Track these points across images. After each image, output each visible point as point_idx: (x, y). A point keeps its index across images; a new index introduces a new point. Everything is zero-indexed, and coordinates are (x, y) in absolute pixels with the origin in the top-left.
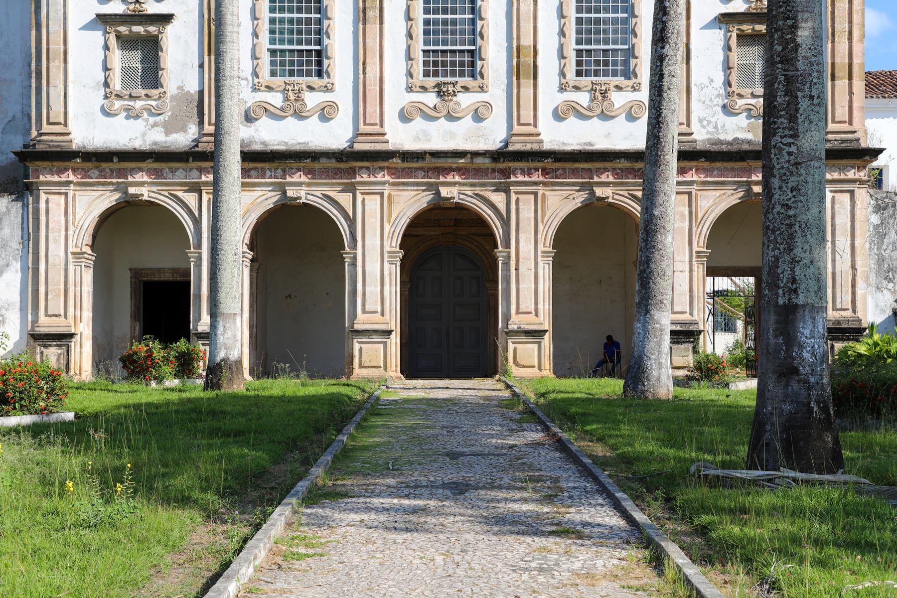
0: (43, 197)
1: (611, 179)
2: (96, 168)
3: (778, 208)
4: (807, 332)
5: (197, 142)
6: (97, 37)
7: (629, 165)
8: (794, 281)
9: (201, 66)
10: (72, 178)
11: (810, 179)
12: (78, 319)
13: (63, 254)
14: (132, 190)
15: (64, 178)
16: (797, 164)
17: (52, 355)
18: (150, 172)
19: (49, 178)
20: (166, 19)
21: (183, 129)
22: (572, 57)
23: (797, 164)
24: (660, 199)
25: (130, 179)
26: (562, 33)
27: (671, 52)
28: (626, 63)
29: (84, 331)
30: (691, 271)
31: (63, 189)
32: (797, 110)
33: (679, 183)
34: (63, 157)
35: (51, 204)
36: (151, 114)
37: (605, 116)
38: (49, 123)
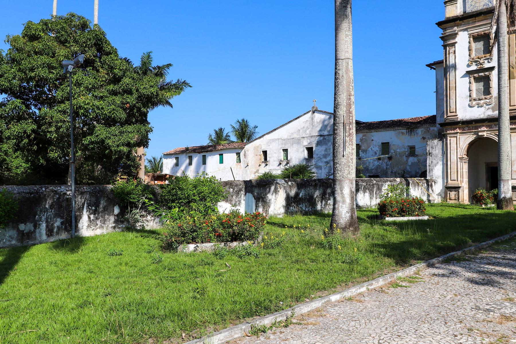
2: (467, 127)
6: (467, 79)
10: (458, 131)
12: (462, 182)
14: (480, 134)
15: (455, 131)
17: (453, 194)
19: (451, 132)
25: (479, 130)
29: (465, 185)
34: (455, 124)
38: (450, 112)
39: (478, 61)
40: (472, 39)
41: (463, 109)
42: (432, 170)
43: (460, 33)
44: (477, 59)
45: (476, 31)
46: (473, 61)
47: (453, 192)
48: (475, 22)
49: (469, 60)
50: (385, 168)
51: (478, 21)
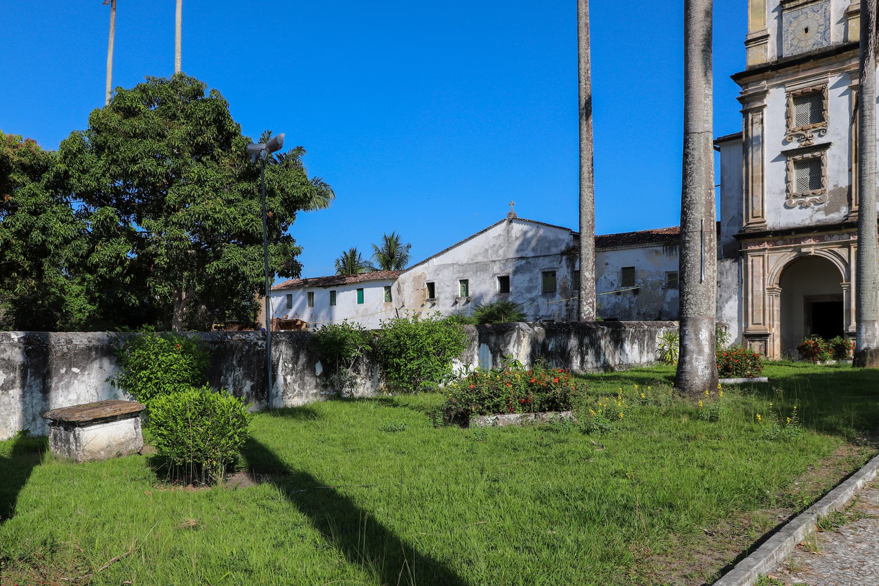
0: (750, 258)
2: (782, 239)
5: (847, 217)
6: (782, 164)
9: (850, 170)
10: (767, 246)
13: (761, 289)
14: (804, 250)
15: (762, 247)
18: (815, 238)
20: (827, 146)
21: (838, 210)
25: (803, 243)
31: (761, 253)
34: (762, 235)
35: (755, 262)
36: (816, 204)
39: (801, 135)
40: (791, 100)
41: (774, 209)
42: (721, 309)
43: (771, 91)
44: (800, 132)
45: (798, 87)
46: (791, 135)
47: (757, 343)
48: (798, 72)
49: (786, 134)
50: (627, 307)
51: (803, 71)
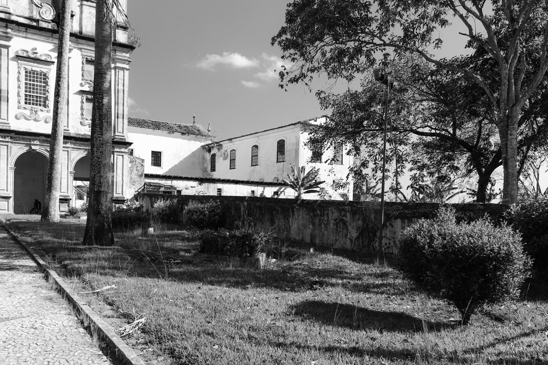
1: (38, 143)
3: (96, 158)
4: (104, 200)
7: (45, 139)
8: (100, 183)
11: (106, 149)
16: (102, 144)
22: (23, 97)
23: (102, 144)
24: (56, 152)
26: (19, 87)
27: (61, 100)
28: (45, 102)
30: (68, 178)
32: (103, 126)
33: (64, 147)
37: (35, 120)
